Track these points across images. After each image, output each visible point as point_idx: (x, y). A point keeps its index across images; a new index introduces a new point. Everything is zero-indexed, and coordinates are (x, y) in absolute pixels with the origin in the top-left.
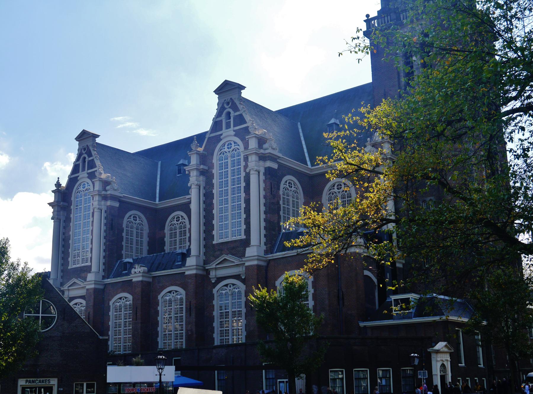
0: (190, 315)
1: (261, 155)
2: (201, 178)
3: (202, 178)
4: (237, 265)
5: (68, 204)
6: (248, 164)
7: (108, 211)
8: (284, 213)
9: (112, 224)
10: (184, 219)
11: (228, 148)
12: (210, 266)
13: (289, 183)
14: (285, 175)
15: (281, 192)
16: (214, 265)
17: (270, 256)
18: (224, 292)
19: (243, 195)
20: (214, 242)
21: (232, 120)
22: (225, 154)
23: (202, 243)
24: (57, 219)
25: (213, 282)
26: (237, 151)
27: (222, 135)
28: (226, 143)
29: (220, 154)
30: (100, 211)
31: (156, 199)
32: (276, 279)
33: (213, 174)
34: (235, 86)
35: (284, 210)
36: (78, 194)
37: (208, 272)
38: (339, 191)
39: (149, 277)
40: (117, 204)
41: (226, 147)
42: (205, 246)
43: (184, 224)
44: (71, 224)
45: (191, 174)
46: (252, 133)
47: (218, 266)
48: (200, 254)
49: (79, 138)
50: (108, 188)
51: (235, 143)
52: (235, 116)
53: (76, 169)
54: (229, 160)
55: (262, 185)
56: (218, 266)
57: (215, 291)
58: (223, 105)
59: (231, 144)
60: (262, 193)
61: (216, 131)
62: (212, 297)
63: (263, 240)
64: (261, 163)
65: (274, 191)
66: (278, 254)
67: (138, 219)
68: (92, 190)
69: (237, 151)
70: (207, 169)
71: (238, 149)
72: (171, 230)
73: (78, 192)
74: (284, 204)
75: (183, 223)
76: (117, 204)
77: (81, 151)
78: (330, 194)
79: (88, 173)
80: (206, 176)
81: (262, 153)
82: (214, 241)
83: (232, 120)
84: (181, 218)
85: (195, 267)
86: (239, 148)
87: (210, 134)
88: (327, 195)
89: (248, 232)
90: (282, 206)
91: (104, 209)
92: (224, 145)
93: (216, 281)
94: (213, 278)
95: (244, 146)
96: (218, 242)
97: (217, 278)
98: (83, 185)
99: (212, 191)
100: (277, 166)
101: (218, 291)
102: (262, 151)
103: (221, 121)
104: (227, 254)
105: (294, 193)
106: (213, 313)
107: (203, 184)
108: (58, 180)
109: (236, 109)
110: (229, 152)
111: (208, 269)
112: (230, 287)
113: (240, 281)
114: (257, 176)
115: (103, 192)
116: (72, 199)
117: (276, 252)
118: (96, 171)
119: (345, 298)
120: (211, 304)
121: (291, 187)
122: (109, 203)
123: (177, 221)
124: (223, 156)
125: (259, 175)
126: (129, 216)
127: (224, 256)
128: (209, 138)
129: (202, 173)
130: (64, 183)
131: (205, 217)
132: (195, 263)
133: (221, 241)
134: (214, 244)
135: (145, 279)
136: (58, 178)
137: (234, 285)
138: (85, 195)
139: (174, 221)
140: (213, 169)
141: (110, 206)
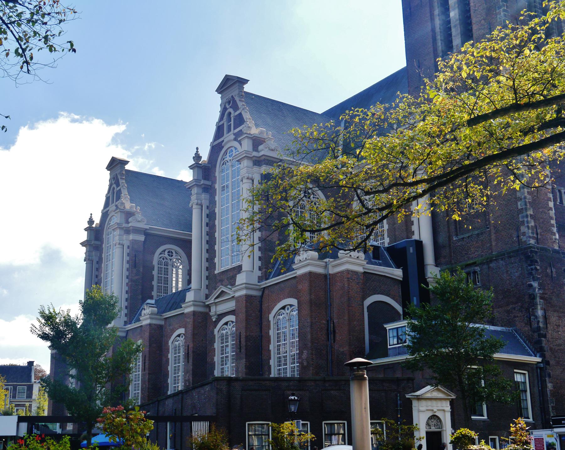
0: (188, 362)
7: (131, 246)
9: (135, 261)
20: (216, 272)
24: (89, 260)
25: (214, 320)
27: (223, 141)
39: (160, 319)
47: (217, 300)
49: (110, 167)
56: (217, 300)
58: (225, 105)
63: (258, 263)
64: (256, 169)
67: (174, 254)
70: (211, 184)
91: (126, 243)
94: (214, 316)
97: (218, 315)
99: (214, 211)
107: (205, 203)
108: (91, 217)
111: (208, 305)
119: (337, 331)
122: (131, 237)
126: (163, 251)
130: (97, 220)
133: (223, 269)
135: (154, 322)
136: (91, 214)
141: (132, 240)
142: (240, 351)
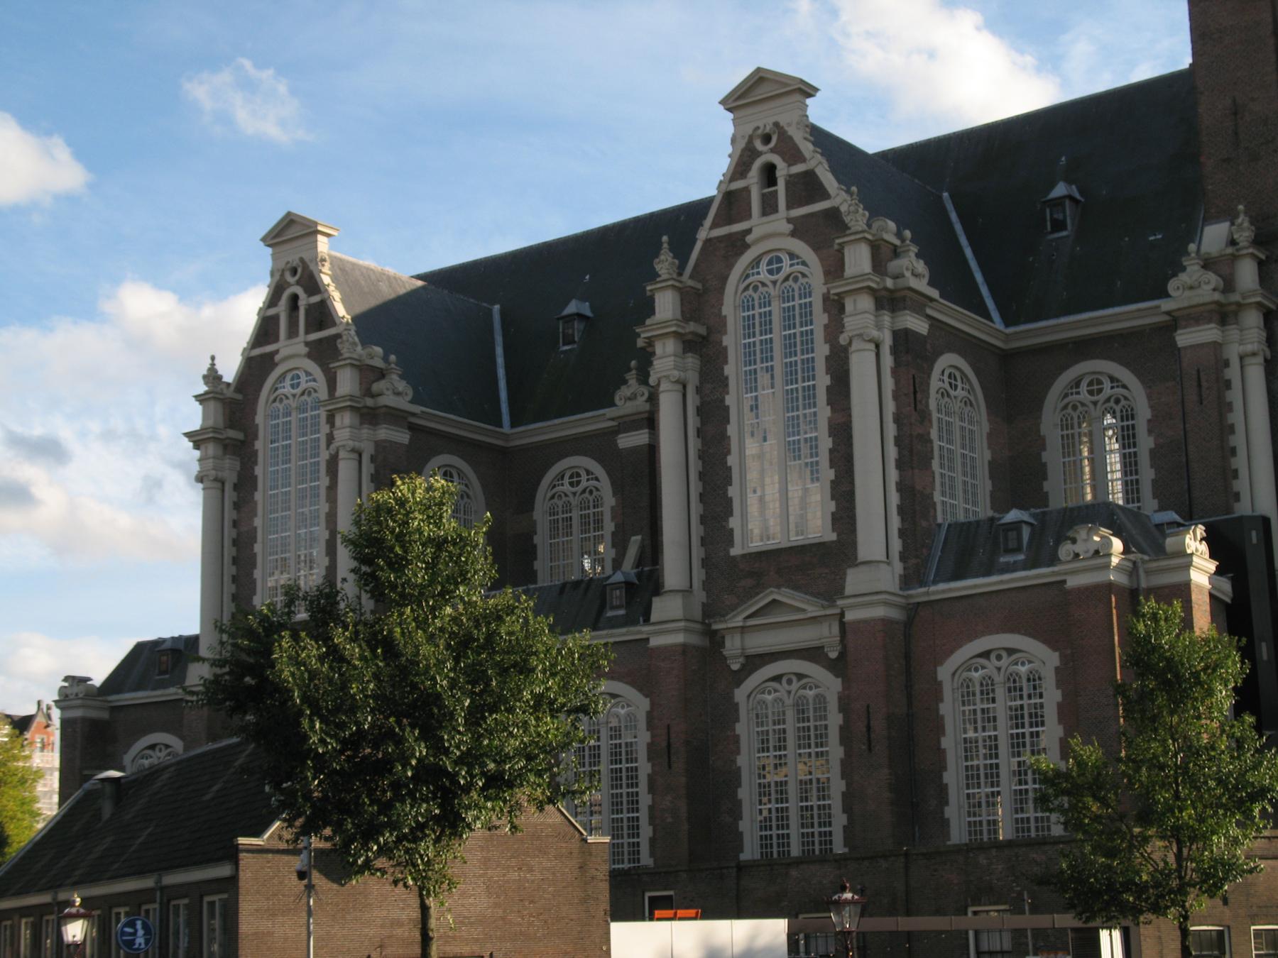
1: (884, 293)
2: (690, 360)
3: (692, 361)
4: (814, 619)
5: (246, 436)
6: (845, 320)
8: (942, 466)
10: (597, 479)
11: (770, 272)
12: (726, 621)
13: (950, 376)
14: (941, 353)
15: (933, 405)
16: (740, 618)
17: (919, 594)
18: (769, 698)
19: (824, 412)
20: (736, 551)
21: (781, 187)
22: (761, 289)
23: (698, 553)
25: (735, 667)
26: (802, 280)
27: (749, 231)
28: (765, 256)
29: (746, 288)
30: (355, 456)
31: (501, 419)
32: (939, 661)
33: (726, 349)
34: (790, 85)
35: (941, 457)
36: (277, 404)
37: (716, 640)
38: (1095, 398)
40: (403, 437)
41: (763, 267)
42: (705, 563)
43: (595, 493)
44: (258, 496)
45: (658, 348)
46: (853, 230)
48: (691, 587)
49: (275, 237)
50: (376, 387)
51: (792, 256)
52: (790, 176)
53: (266, 330)
54: (776, 308)
55: (889, 383)
57: (740, 694)
58: (751, 140)
59: (779, 260)
60: (890, 407)
61: (730, 221)
62: (730, 713)
63: (897, 545)
64: (886, 318)
65: (920, 402)
66: (942, 586)
68: (323, 394)
69: (802, 280)
71: (804, 275)
72: (553, 513)
73: (274, 401)
74: (940, 438)
75: (591, 492)
76: (403, 437)
77: (282, 275)
78: (1065, 407)
79: (307, 344)
80: (701, 356)
81: (886, 289)
82: (733, 546)
83: (781, 187)
84: (584, 477)
85: (682, 624)
86: (807, 273)
87: (711, 228)
88: (1058, 410)
89: (845, 516)
90: (936, 443)
91: (368, 449)
92: (756, 262)
93: (743, 666)
94: (736, 657)
95: (823, 266)
96: (745, 552)
97: (747, 657)
98: (292, 379)
99: (723, 400)
100: (927, 326)
101: (749, 696)
102: (889, 283)
103: (747, 190)
104: (778, 587)
105: (963, 404)
106: (734, 761)
107: (693, 379)
109: (794, 155)
110: (774, 283)
111: (716, 631)
112: (790, 682)
113: (823, 667)
114: (872, 356)
115: (369, 402)
116: (259, 419)
117: (935, 582)
118: (338, 336)
120: (729, 733)
121: (956, 387)
122: (385, 433)
123: (571, 484)
124: (756, 296)
125: (878, 355)
127: (772, 592)
128: (708, 242)
129: (691, 344)
130: (230, 370)
131: (702, 476)
132: (679, 613)
134: (734, 558)
136: (213, 358)
137: (800, 676)
138: (302, 409)
139: (562, 485)
140: (725, 333)
141: (385, 441)
142: (870, 750)
